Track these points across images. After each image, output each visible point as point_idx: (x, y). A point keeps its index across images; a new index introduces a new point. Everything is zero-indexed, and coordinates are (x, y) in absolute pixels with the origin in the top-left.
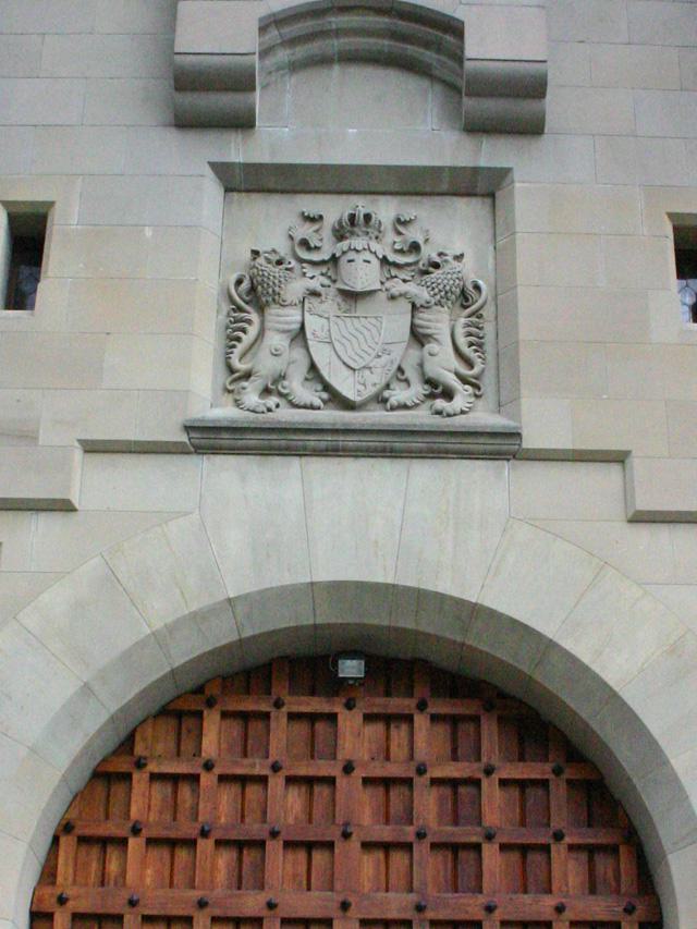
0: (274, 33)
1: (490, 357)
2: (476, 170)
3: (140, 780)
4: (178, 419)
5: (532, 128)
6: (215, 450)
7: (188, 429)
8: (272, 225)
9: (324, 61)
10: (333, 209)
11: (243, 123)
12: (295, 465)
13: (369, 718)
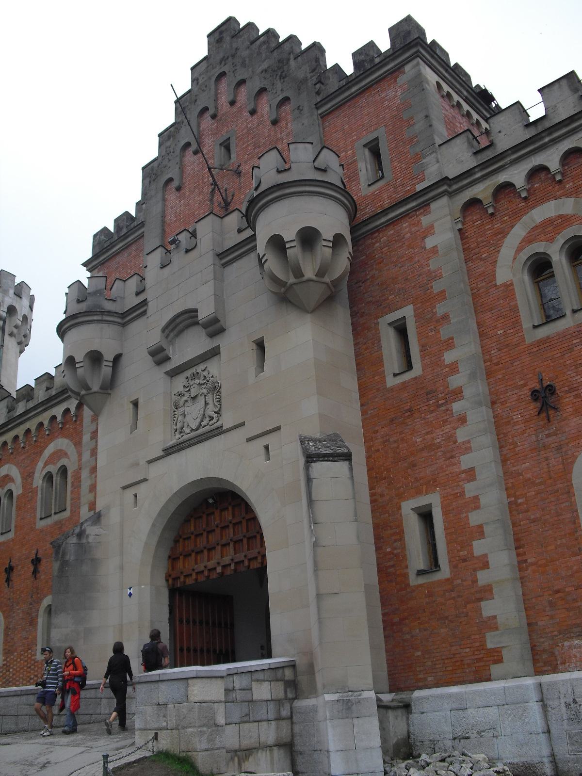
0: (167, 331)
1: (222, 404)
2: (213, 349)
3: (181, 540)
4: (162, 447)
5: (222, 330)
6: (170, 454)
7: (163, 451)
8: (180, 382)
9: (182, 331)
10: (188, 373)
11: (168, 359)
12: (183, 452)
13: (222, 510)
